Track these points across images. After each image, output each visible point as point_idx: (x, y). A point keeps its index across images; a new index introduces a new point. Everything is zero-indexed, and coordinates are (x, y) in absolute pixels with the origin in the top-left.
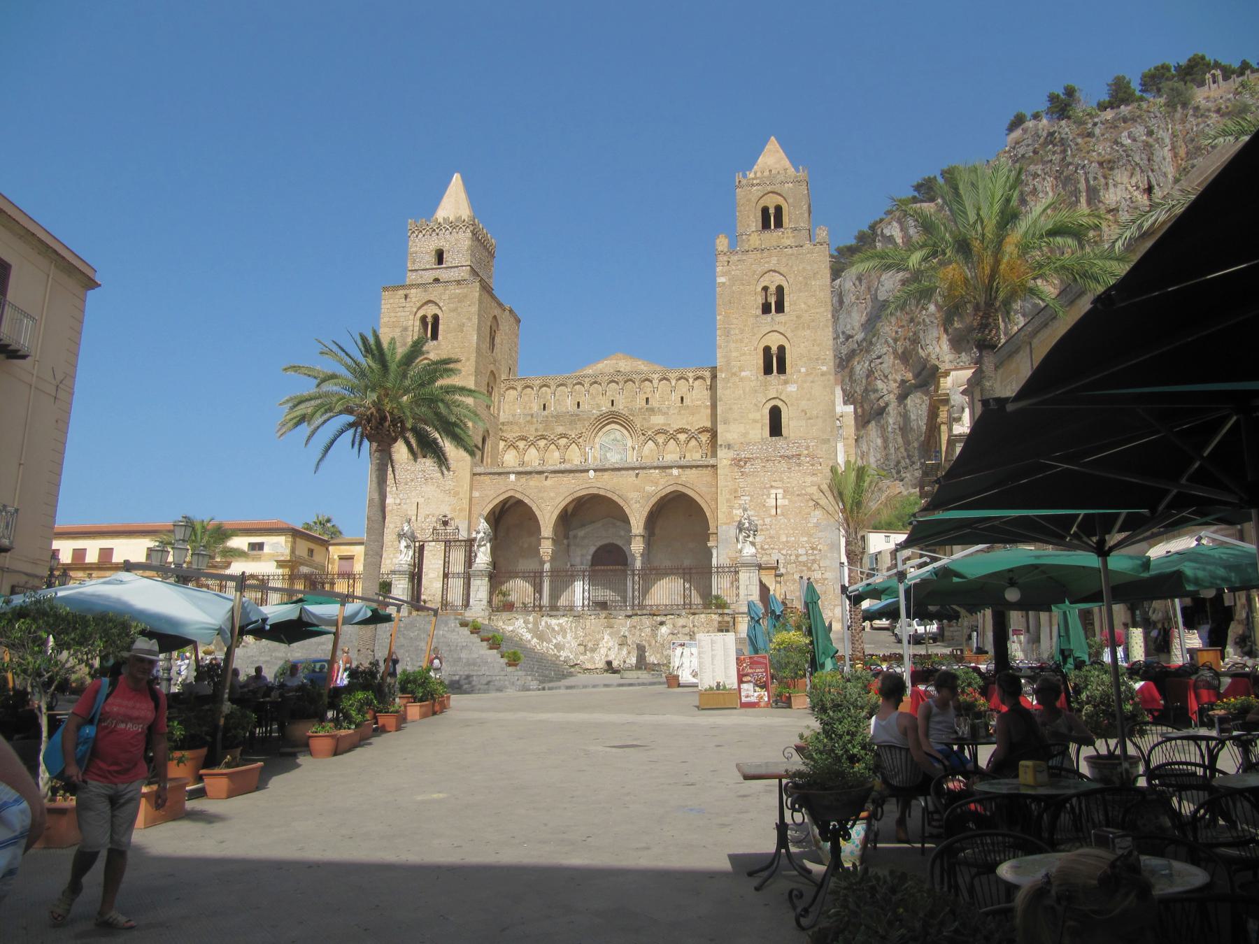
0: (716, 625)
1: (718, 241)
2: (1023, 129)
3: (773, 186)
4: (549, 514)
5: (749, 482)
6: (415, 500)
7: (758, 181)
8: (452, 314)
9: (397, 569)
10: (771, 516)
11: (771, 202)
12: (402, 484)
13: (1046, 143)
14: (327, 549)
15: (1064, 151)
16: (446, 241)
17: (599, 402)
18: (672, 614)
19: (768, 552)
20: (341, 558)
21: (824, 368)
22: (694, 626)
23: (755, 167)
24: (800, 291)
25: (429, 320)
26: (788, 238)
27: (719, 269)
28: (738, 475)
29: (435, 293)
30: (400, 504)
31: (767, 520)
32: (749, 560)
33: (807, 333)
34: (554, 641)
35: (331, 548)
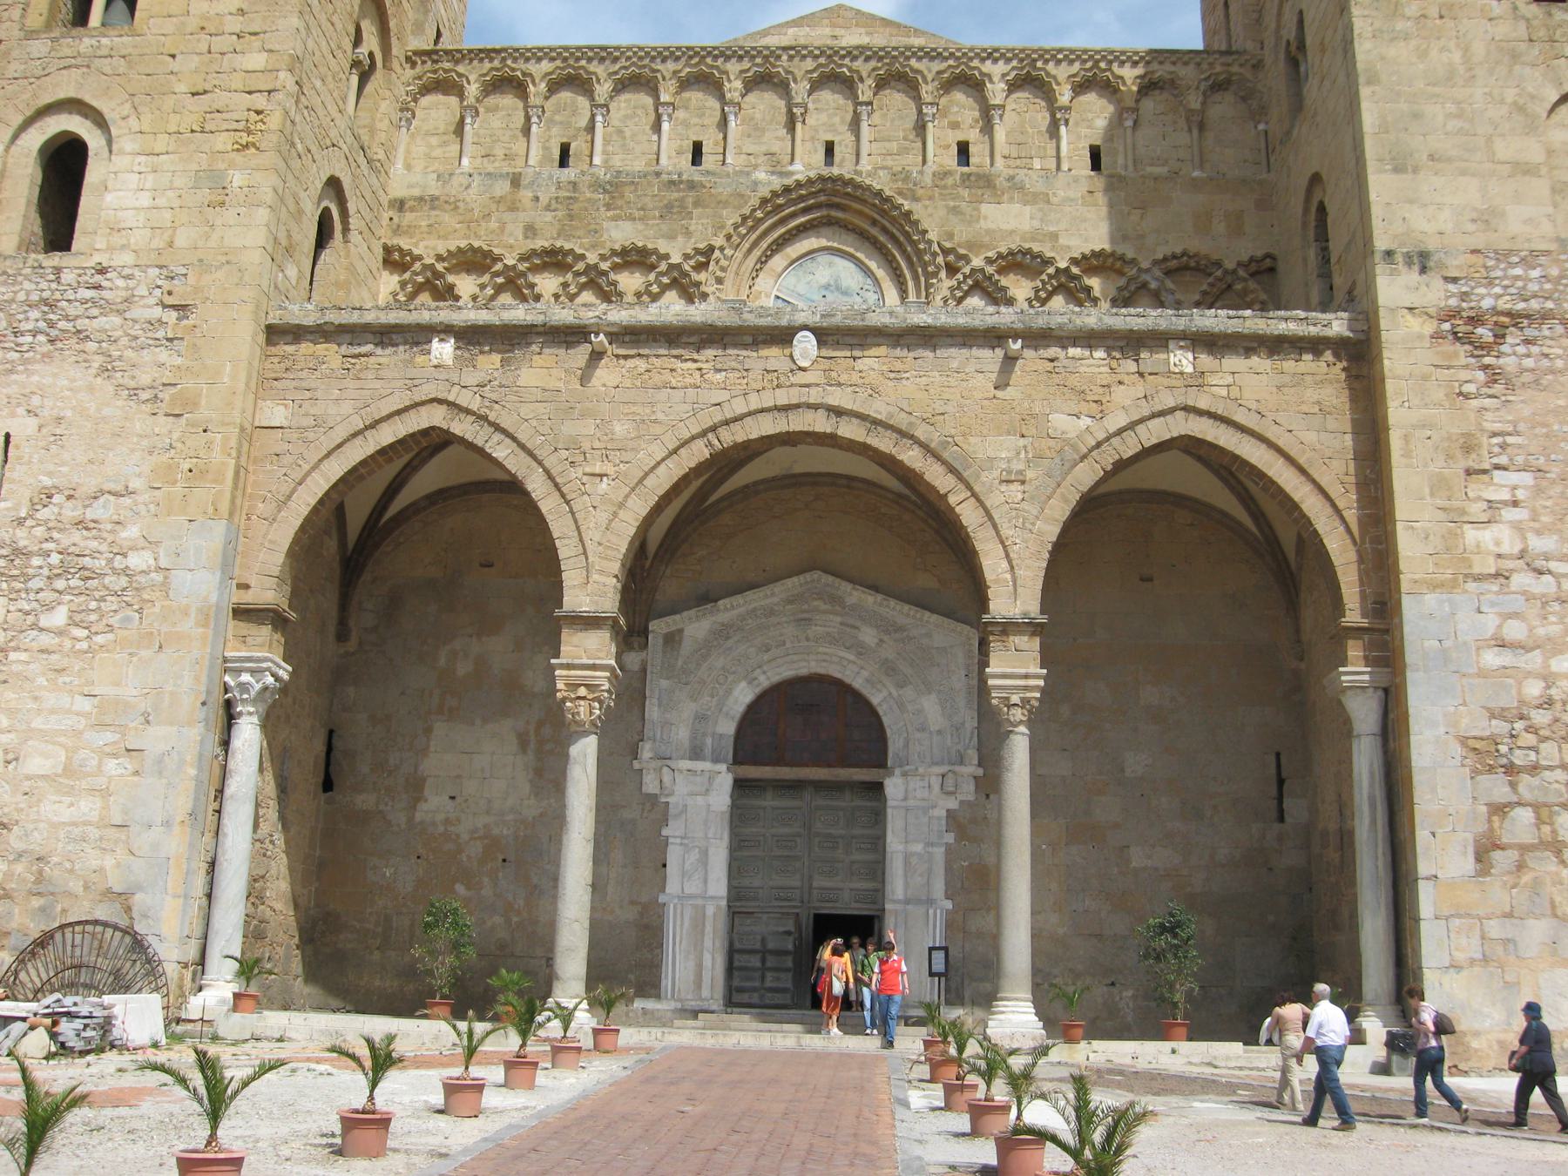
4: (603, 516)
5: (1526, 411)
17: (775, 148)
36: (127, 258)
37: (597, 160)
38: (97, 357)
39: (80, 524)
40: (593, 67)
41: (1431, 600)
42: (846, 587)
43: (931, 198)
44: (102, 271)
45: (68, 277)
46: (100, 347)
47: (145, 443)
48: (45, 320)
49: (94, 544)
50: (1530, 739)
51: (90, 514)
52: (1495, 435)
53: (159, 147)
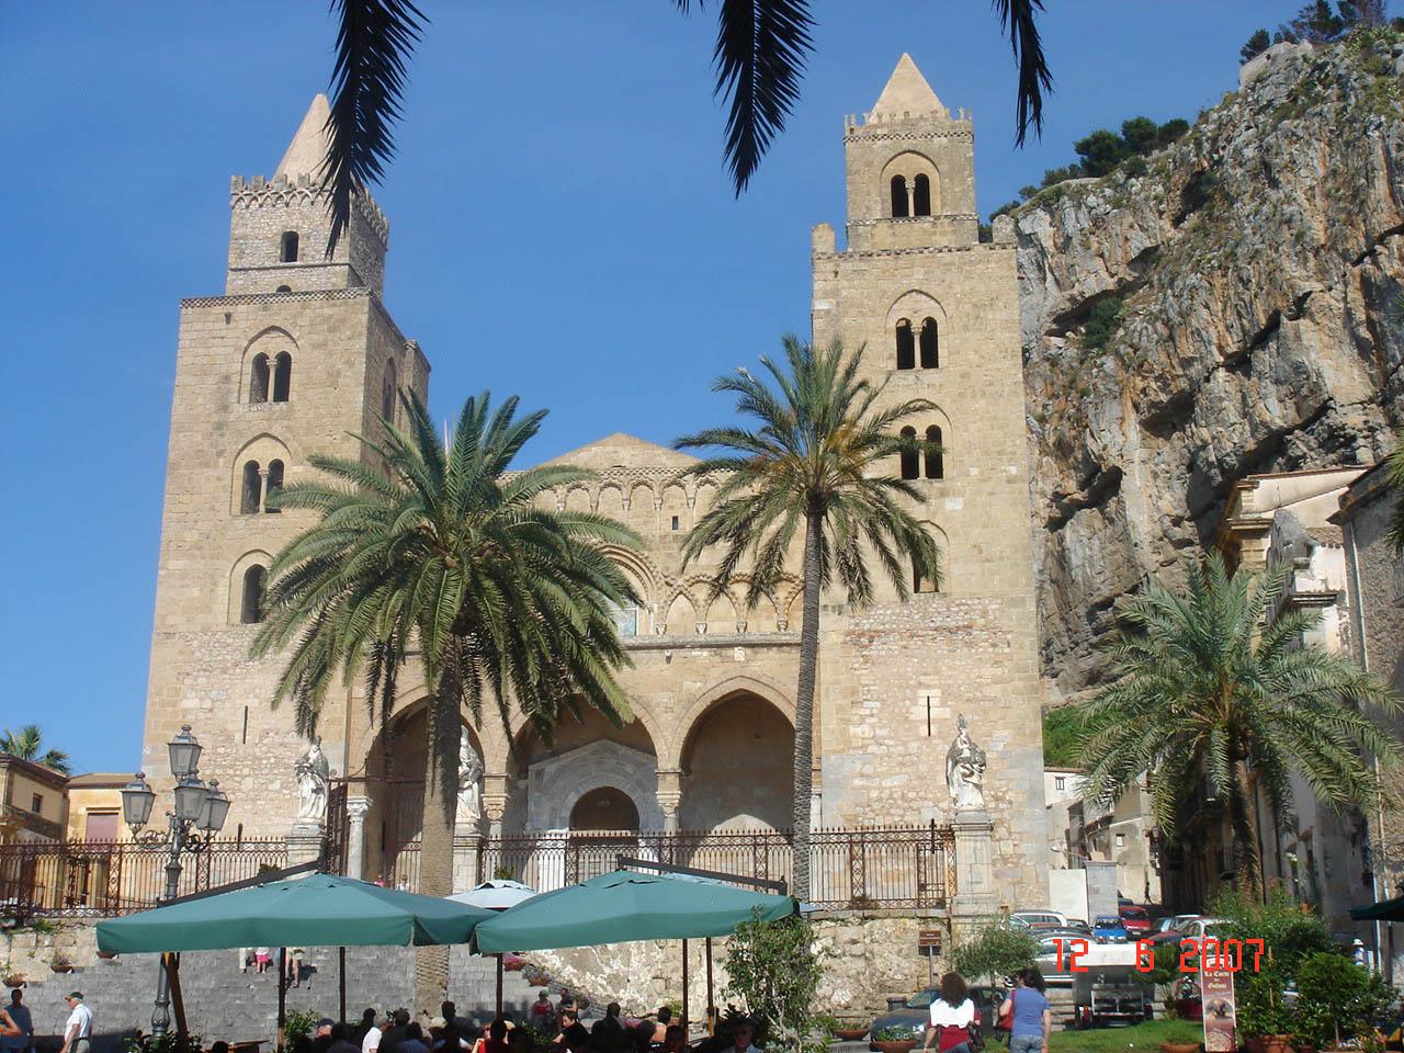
0: (915, 938)
1: (816, 235)
2: (1268, 57)
3: (912, 141)
6: (241, 703)
7: (885, 131)
8: (317, 353)
9: (297, 833)
10: (919, 739)
11: (909, 168)
13: (1308, 85)
14: (65, 796)
15: (1343, 97)
16: (304, 217)
18: (832, 920)
19: (915, 805)
20: (93, 813)
21: (1013, 470)
22: (872, 941)
23: (877, 105)
24: (966, 328)
25: (272, 363)
26: (943, 234)
27: (818, 286)
28: (857, 663)
29: (282, 312)
30: (211, 710)
31: (914, 746)
32: (971, 817)
33: (981, 404)
34: (607, 970)
35: (72, 793)
41: (833, 757)
42: (619, 746)
43: (658, 549)
50: (872, 815)
52: (864, 686)
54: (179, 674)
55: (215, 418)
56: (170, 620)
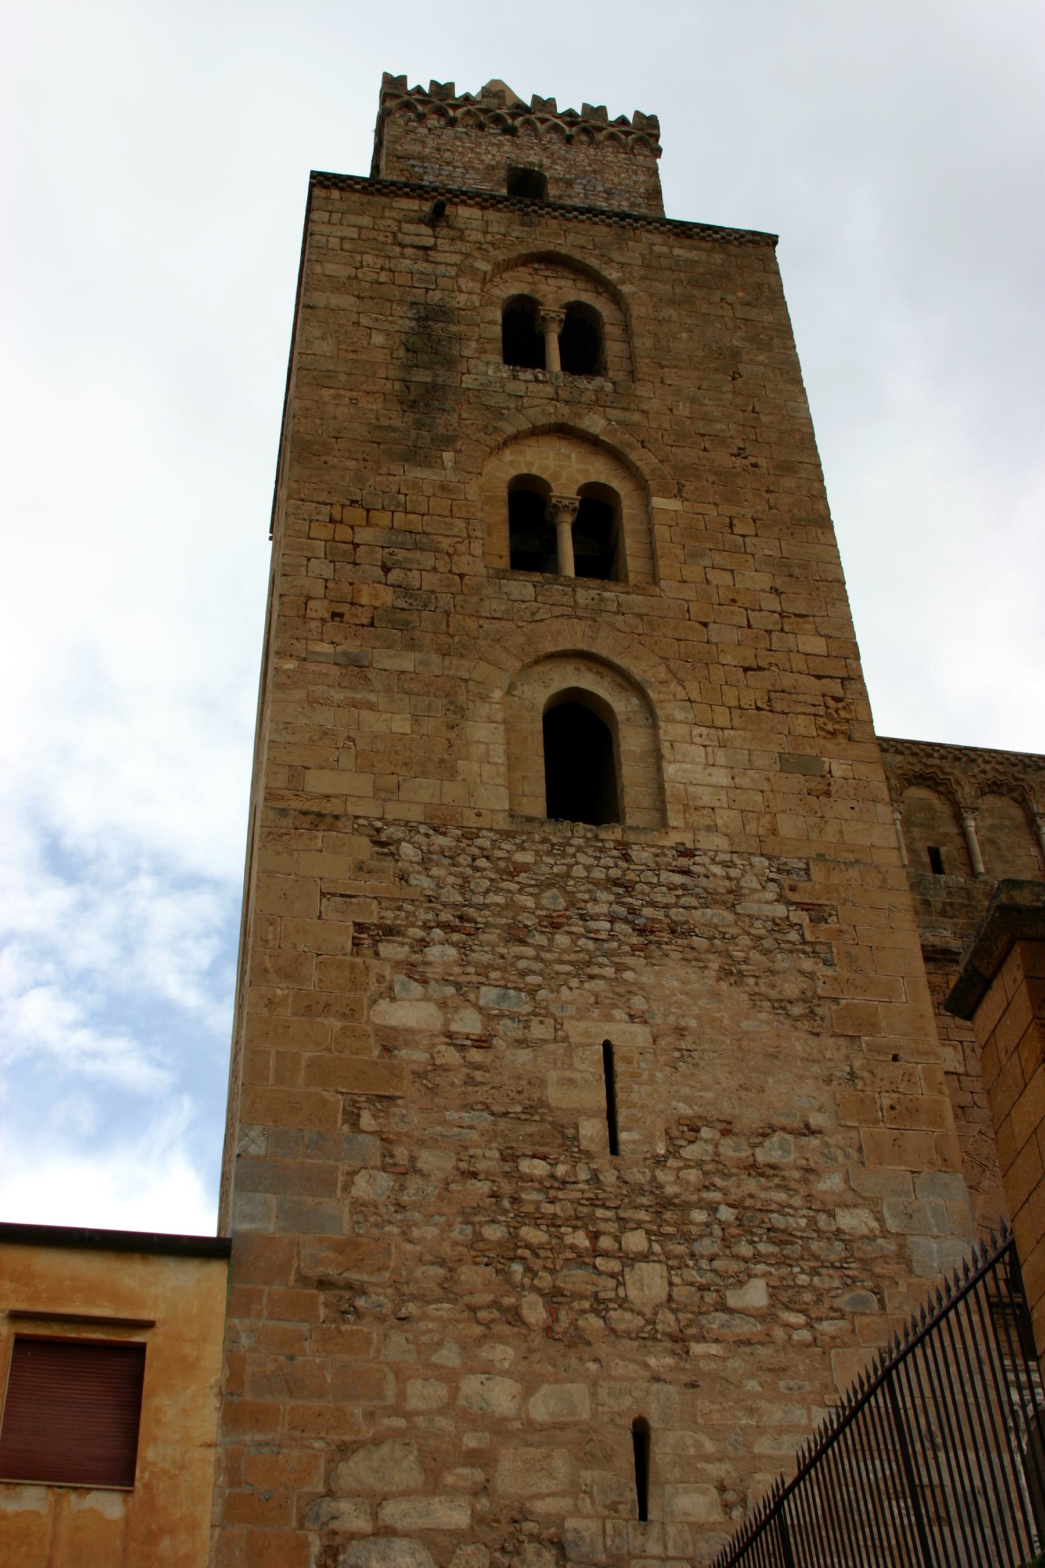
12: (491, 936)
30: (482, 1043)
36: (718, 842)
37: (981, 868)
38: (710, 956)
39: (753, 1168)
40: (945, 764)
44: (689, 854)
45: (641, 855)
46: (712, 945)
47: (815, 1069)
48: (623, 904)
49: (781, 1196)
51: (761, 1157)
53: (722, 719)
54: (360, 927)
55: (422, 376)
56: (318, 782)
